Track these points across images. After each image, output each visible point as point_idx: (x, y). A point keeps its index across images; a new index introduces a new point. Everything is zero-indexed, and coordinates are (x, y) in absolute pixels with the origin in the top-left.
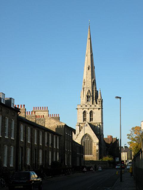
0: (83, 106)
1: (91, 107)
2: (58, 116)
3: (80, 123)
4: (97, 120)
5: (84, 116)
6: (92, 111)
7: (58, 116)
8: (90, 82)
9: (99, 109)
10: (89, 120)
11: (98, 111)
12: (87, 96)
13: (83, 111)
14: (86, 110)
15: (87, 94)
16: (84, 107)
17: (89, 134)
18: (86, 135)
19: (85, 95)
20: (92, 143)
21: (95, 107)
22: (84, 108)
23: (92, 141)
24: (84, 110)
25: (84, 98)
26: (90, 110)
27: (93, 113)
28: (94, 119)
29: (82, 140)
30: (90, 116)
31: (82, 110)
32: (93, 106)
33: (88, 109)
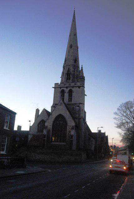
1: (70, 86)
4: (75, 100)
8: (72, 59)
9: (79, 87)
10: (67, 100)
13: (60, 90)
14: (65, 89)
15: (67, 72)
16: (63, 85)
18: (60, 117)
19: (65, 73)
20: (66, 128)
23: (67, 124)
24: (62, 89)
26: (69, 89)
27: (72, 93)
28: (72, 101)
29: (54, 122)
32: (73, 84)
33: (67, 88)
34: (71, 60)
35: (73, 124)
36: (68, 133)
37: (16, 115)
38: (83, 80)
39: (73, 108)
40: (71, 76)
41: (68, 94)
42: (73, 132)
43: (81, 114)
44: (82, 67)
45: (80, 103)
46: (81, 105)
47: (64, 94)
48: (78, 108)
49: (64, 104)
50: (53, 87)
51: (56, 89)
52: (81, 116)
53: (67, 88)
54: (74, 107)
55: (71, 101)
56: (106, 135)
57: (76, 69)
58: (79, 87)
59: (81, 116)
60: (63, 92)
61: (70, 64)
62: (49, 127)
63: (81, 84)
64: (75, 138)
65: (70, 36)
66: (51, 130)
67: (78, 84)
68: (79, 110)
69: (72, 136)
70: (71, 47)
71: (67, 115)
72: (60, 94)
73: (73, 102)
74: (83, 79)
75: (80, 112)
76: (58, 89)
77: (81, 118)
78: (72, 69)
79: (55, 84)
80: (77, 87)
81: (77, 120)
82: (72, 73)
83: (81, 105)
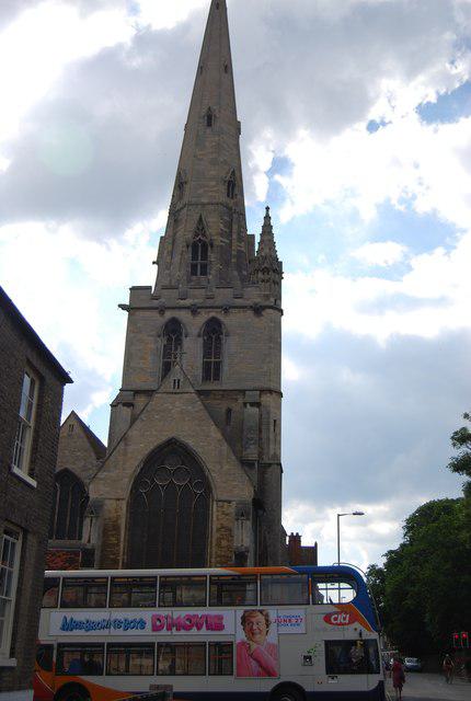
3: (137, 392)
5: (167, 352)
9: (258, 310)
10: (199, 372)
11: (257, 320)
12: (195, 246)
13: (160, 320)
14: (184, 316)
15: (190, 236)
16: (170, 297)
17: (190, 442)
18: (172, 453)
20: (206, 507)
21: (239, 302)
22: (168, 304)
24: (169, 315)
25: (177, 259)
26: (203, 317)
29: (138, 481)
30: (207, 354)
31: (155, 314)
32: (223, 296)
33: (194, 310)
34: (213, 183)
35: (246, 493)
36: (219, 540)
37: (67, 387)
38: (272, 275)
39: (229, 411)
40: (212, 256)
41: (201, 340)
43: (272, 446)
44: (267, 228)
45: (262, 391)
46: (267, 399)
47: (179, 342)
51: (140, 314)
52: (272, 452)
53: (194, 310)
54: (236, 407)
55: (217, 377)
57: (235, 227)
58: (258, 310)
59: (272, 452)
60: (173, 331)
61: (205, 200)
62: (110, 505)
63: (267, 297)
65: (201, 69)
66: (123, 523)
67: (254, 295)
68: (260, 424)
70: (209, 124)
71: (207, 443)
72: (162, 342)
73: (227, 381)
74: (271, 271)
75: (264, 435)
76: (148, 314)
77: (270, 465)
78: (214, 226)
79: (133, 289)
81: (255, 474)
82: (218, 240)
83: (267, 399)
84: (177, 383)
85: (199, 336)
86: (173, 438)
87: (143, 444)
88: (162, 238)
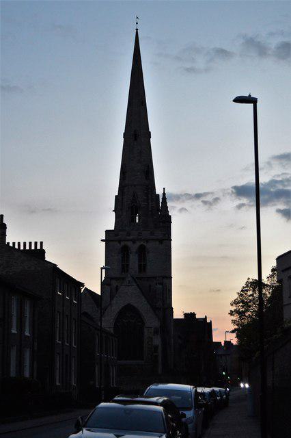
0: (121, 233)
2: (39, 247)
3: (112, 279)
6: (145, 247)
7: (39, 247)
9: (161, 241)
13: (119, 246)
14: (129, 244)
17: (135, 305)
18: (129, 309)
24: (122, 243)
26: (138, 244)
30: (140, 260)
33: (134, 241)
34: (139, 173)
39: (150, 286)
42: (157, 341)
44: (164, 194)
48: (161, 286)
49: (135, 284)
50: (102, 240)
56: (208, 321)
58: (161, 241)
60: (125, 251)
61: (135, 183)
63: (165, 235)
64: (160, 349)
69: (156, 347)
70: (136, 140)
71: (141, 304)
77: (167, 308)
80: (153, 240)
84: (129, 282)
85: (136, 253)
86: (129, 304)
87: (117, 305)
88: (116, 196)
